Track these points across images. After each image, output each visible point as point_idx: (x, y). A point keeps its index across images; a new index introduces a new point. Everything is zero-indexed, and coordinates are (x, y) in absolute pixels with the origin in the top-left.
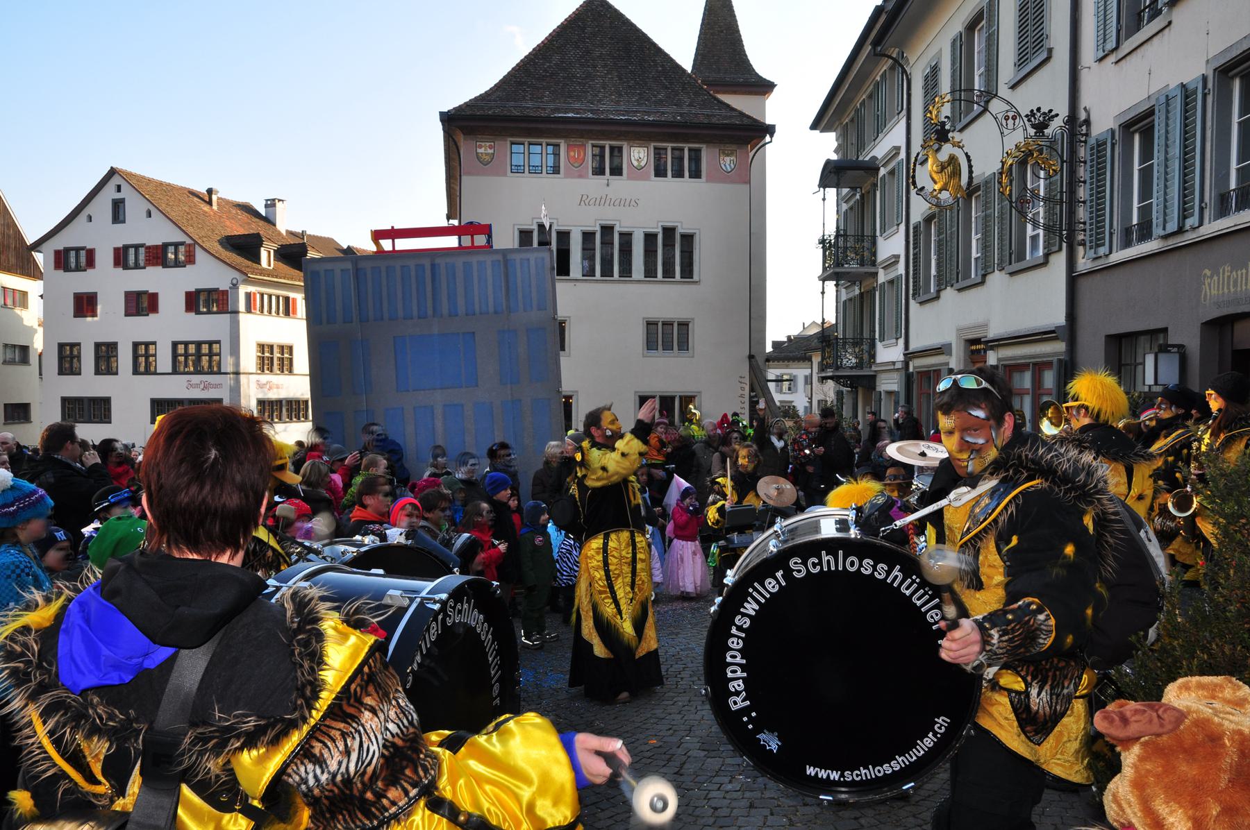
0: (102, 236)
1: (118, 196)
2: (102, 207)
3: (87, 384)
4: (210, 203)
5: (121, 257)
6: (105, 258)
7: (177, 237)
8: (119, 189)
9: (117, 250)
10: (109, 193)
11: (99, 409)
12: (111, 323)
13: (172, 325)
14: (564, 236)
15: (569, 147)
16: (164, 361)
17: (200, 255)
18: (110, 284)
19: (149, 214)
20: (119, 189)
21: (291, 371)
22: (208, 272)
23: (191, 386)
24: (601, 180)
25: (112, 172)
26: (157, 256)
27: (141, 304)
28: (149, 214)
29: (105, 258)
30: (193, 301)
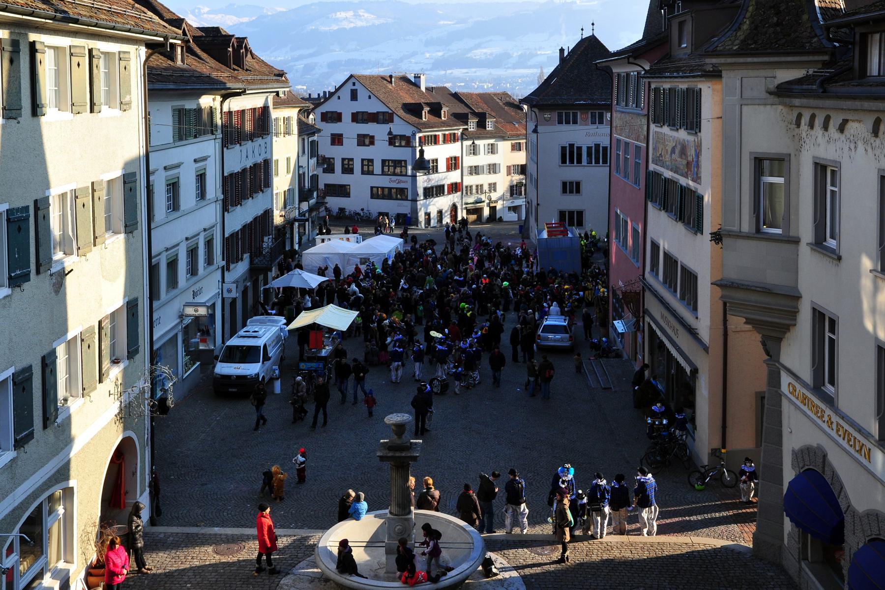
0: (346, 107)
1: (354, 88)
2: (346, 93)
3: (337, 178)
4: (391, 82)
5: (357, 117)
6: (347, 117)
7: (383, 109)
8: (354, 84)
9: (353, 114)
10: (349, 86)
11: (342, 191)
12: (351, 149)
13: (381, 151)
14: (579, 149)
15: (581, 114)
16: (377, 168)
17: (396, 118)
18: (350, 130)
19: (370, 97)
20: (354, 84)
21: (437, 171)
22: (399, 127)
23: (391, 181)
24: (595, 126)
25: (351, 76)
26: (373, 118)
27: (365, 140)
28: (370, 97)
29: (347, 117)
30: (392, 140)
